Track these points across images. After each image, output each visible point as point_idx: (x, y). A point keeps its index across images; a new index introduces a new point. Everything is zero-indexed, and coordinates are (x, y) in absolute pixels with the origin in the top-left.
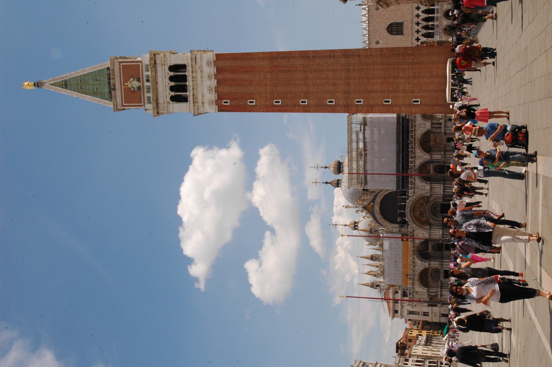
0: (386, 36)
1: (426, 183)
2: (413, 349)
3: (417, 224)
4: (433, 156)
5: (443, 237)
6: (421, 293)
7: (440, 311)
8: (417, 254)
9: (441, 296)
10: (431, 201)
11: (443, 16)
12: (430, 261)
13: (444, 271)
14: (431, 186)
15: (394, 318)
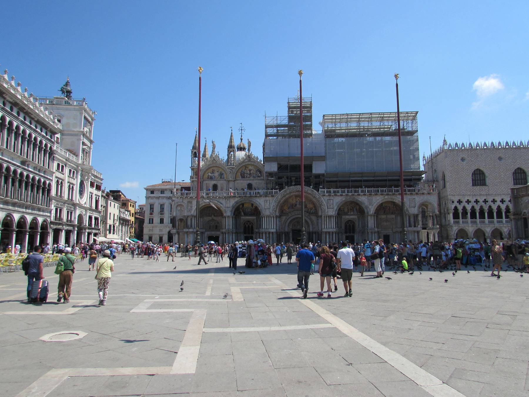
0: (471, 168)
1: (336, 210)
2: (114, 203)
3: (282, 201)
4: (373, 217)
5: (266, 233)
6: (189, 207)
7: (155, 234)
8: (241, 201)
9: (187, 232)
10: (311, 219)
11: (495, 227)
12: (233, 217)
13: (217, 235)
14: (333, 216)
15: (146, 190)
